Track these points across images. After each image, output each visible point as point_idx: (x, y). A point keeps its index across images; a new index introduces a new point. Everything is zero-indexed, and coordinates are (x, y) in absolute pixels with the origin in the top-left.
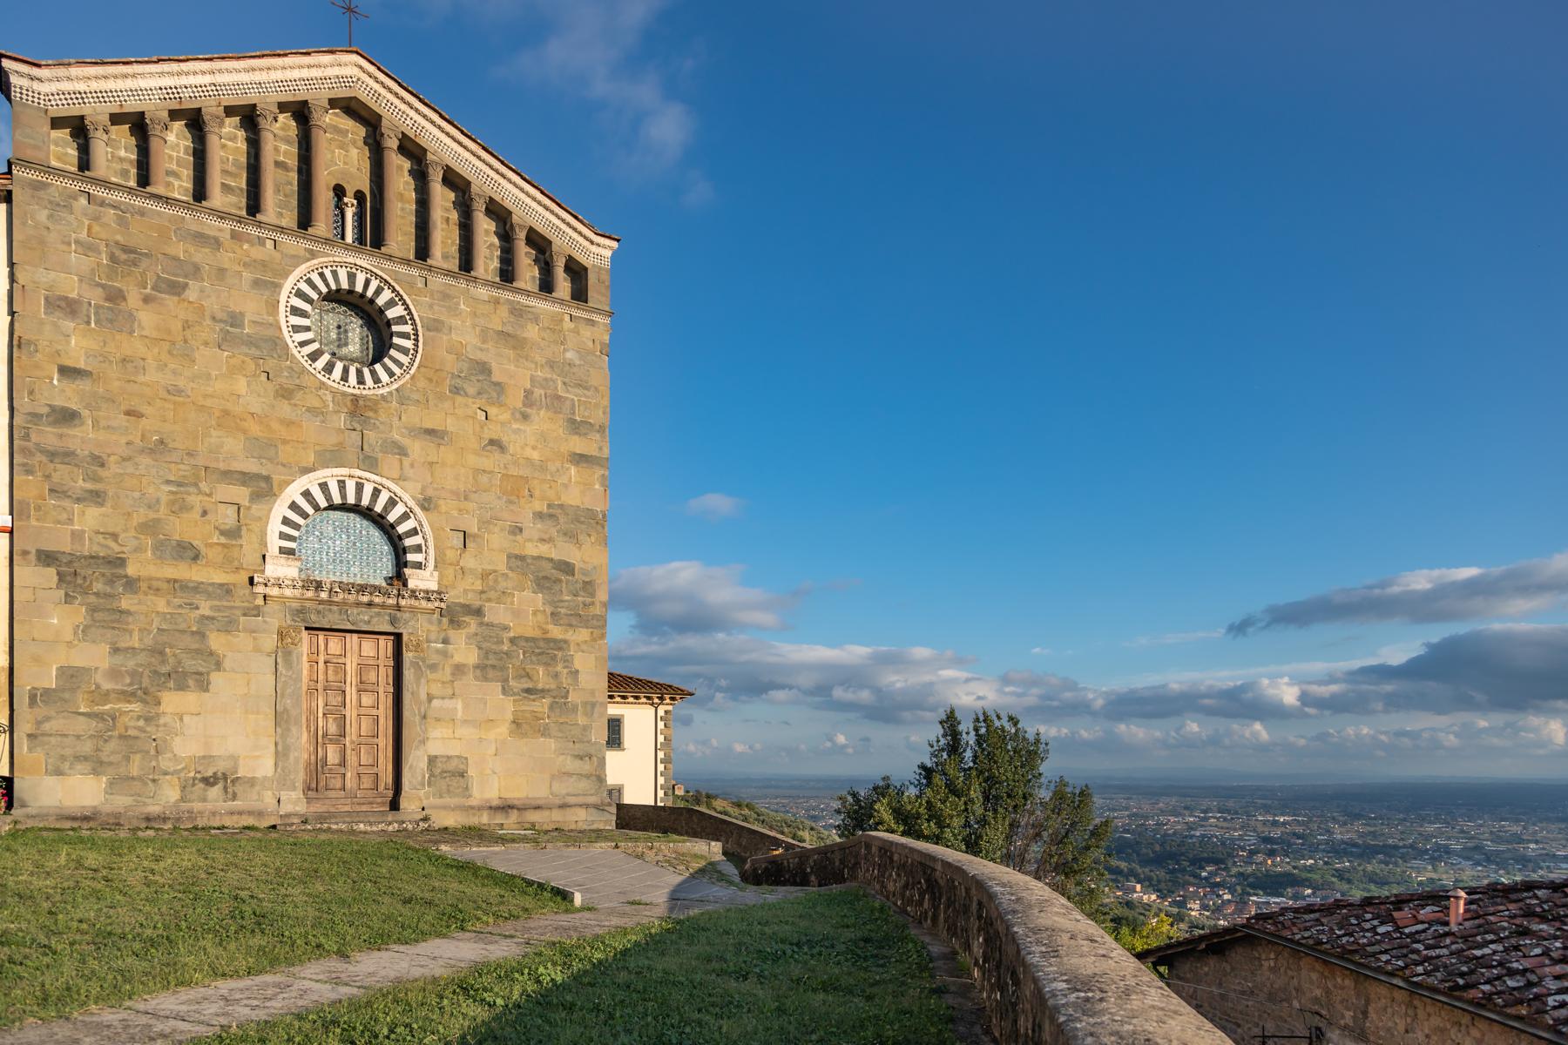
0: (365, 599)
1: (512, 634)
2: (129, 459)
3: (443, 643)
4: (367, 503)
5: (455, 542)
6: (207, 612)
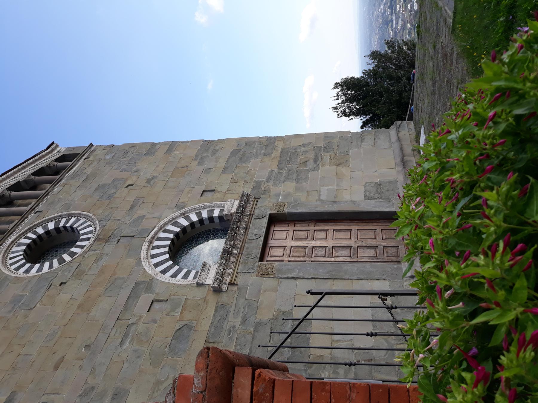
0: (242, 231)
1: (276, 169)
2: (93, 369)
3: (279, 196)
4: (173, 235)
5: (210, 195)
6: (239, 320)
